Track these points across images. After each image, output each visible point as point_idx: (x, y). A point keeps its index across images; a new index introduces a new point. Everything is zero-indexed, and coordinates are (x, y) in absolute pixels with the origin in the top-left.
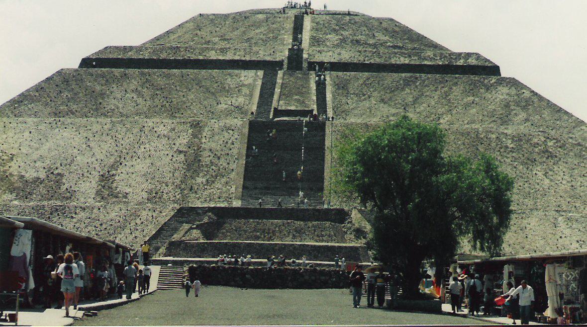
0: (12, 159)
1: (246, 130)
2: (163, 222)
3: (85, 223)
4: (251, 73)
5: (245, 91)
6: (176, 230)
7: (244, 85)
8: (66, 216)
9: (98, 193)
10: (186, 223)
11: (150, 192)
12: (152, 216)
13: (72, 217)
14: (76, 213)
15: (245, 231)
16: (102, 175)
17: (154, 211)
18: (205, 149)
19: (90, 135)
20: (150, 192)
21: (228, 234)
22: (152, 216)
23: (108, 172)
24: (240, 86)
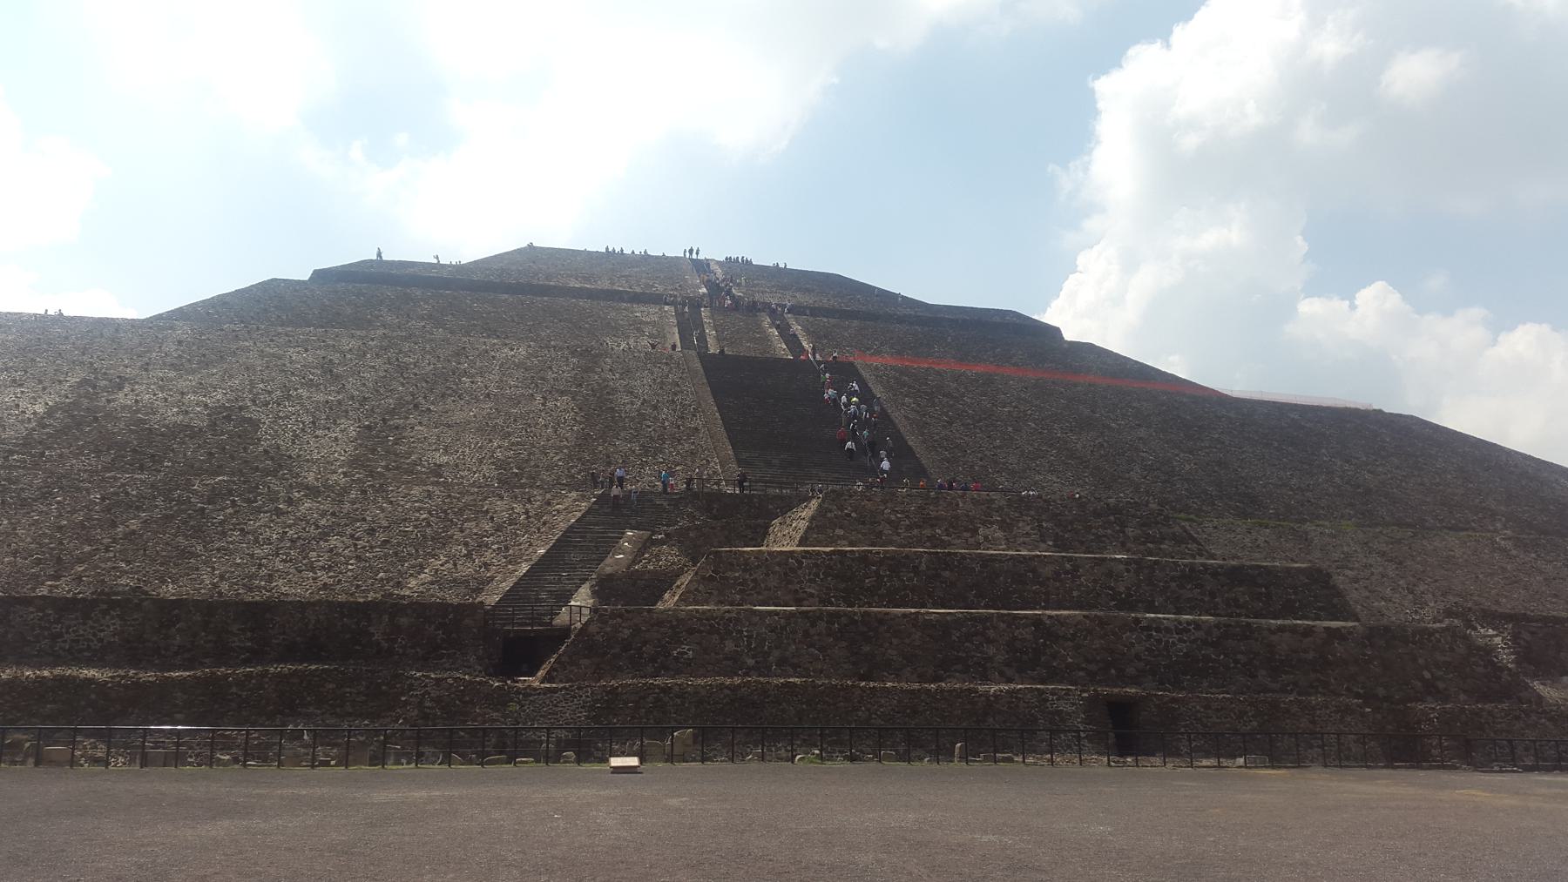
0: (121, 388)
1: (697, 365)
2: (563, 526)
3: (318, 527)
4: (654, 309)
5: (647, 330)
6: (609, 545)
7: (642, 322)
8: (260, 507)
9: (354, 462)
10: (632, 529)
11: (501, 465)
12: (527, 512)
13: (279, 512)
14: (290, 502)
15: (895, 525)
16: (369, 428)
17: (529, 501)
18: (615, 390)
19: (336, 357)
20: (501, 465)
21: (839, 532)
22: (527, 512)
23: (384, 420)
24: (638, 326)
